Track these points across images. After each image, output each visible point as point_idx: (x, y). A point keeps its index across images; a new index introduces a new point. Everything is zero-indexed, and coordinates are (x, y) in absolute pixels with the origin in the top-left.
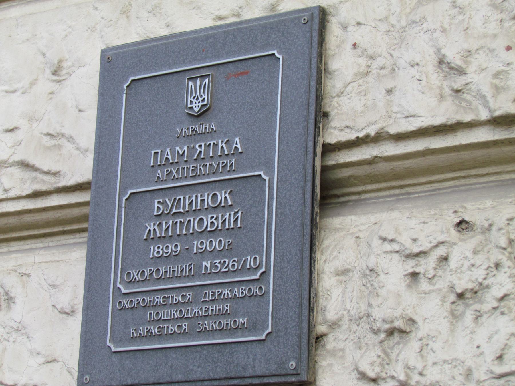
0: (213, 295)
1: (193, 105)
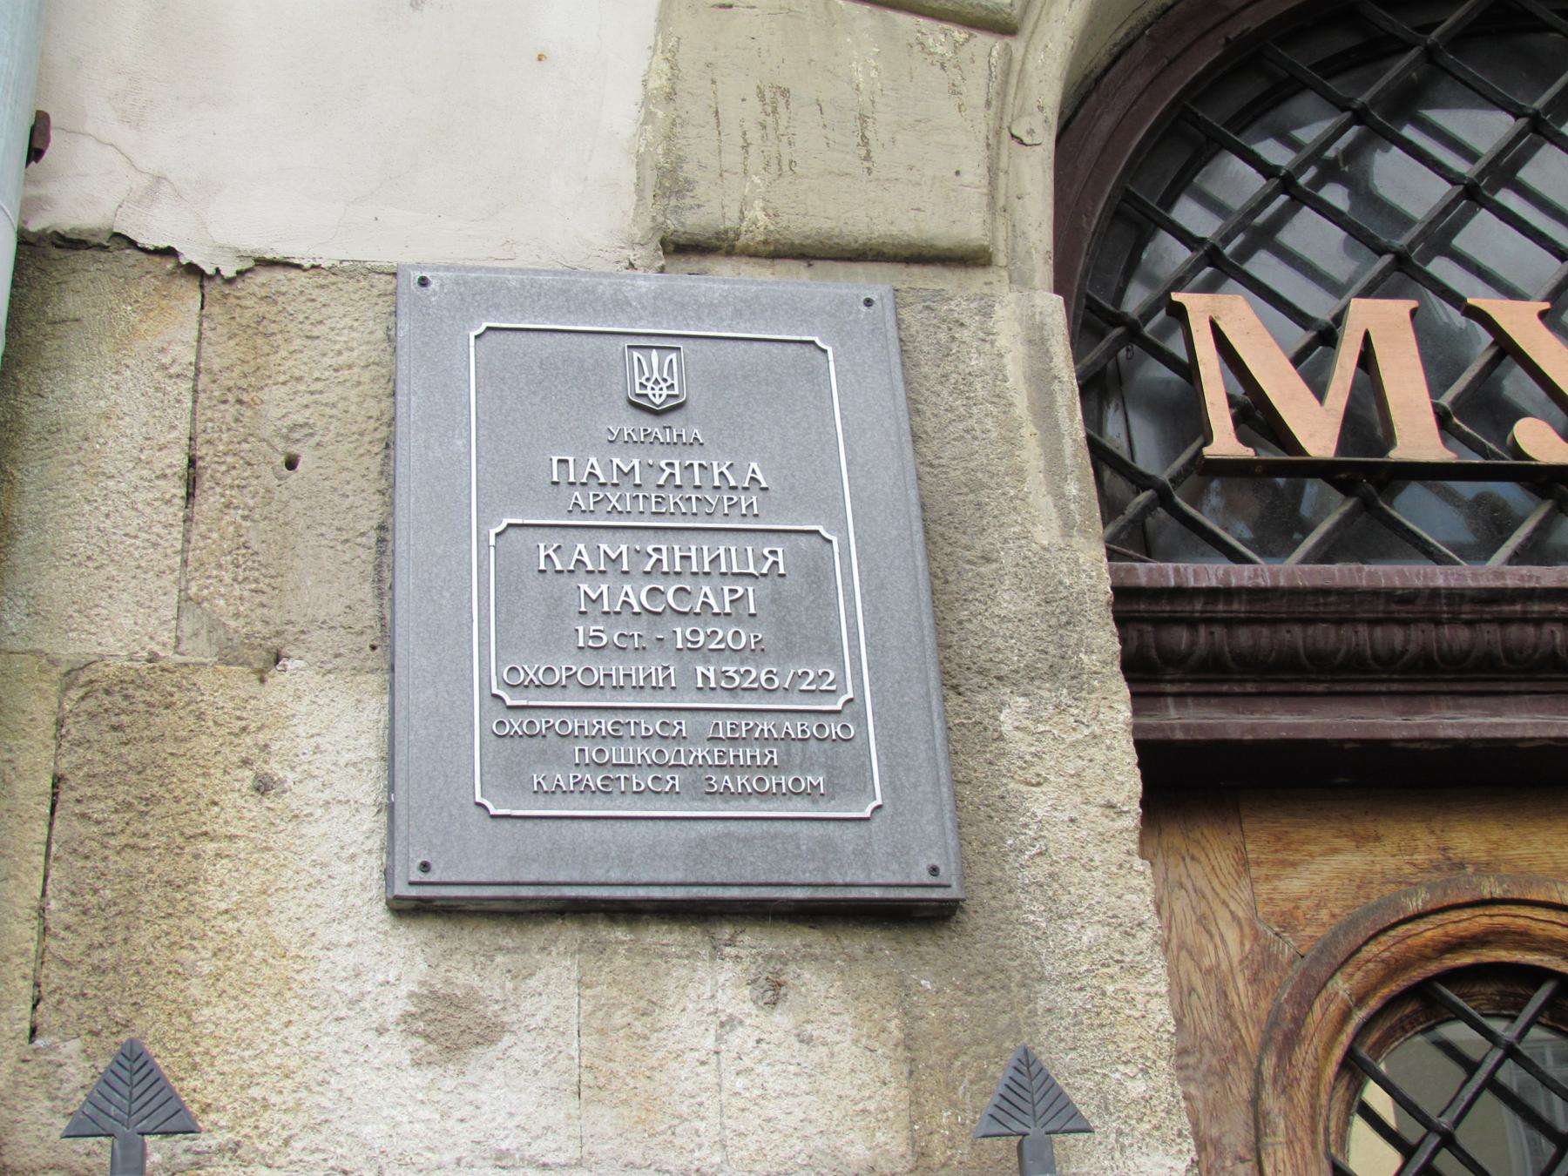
1: (649, 392)
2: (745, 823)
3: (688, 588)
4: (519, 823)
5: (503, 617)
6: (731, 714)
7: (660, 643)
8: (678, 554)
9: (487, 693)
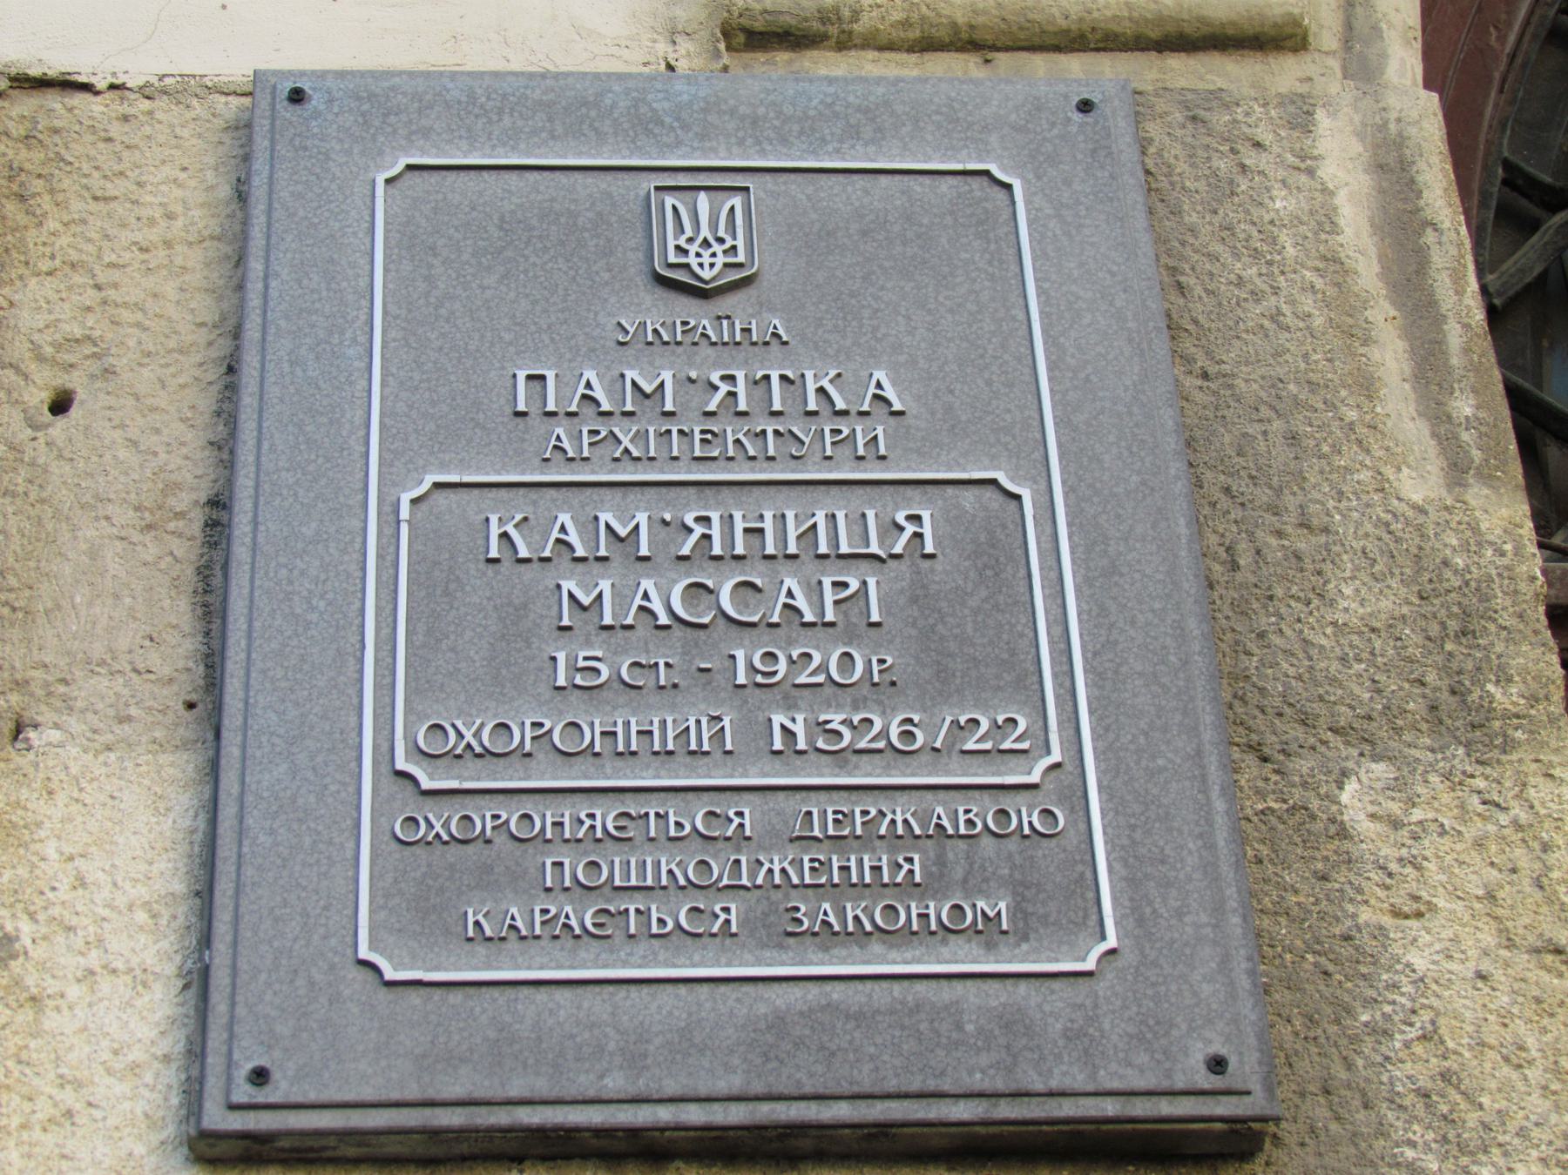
0: (842, 819)
1: (692, 260)
2: (859, 985)
3: (758, 582)
4: (438, 993)
5: (419, 639)
6: (835, 795)
7: (704, 677)
8: (739, 526)
9: (385, 769)
